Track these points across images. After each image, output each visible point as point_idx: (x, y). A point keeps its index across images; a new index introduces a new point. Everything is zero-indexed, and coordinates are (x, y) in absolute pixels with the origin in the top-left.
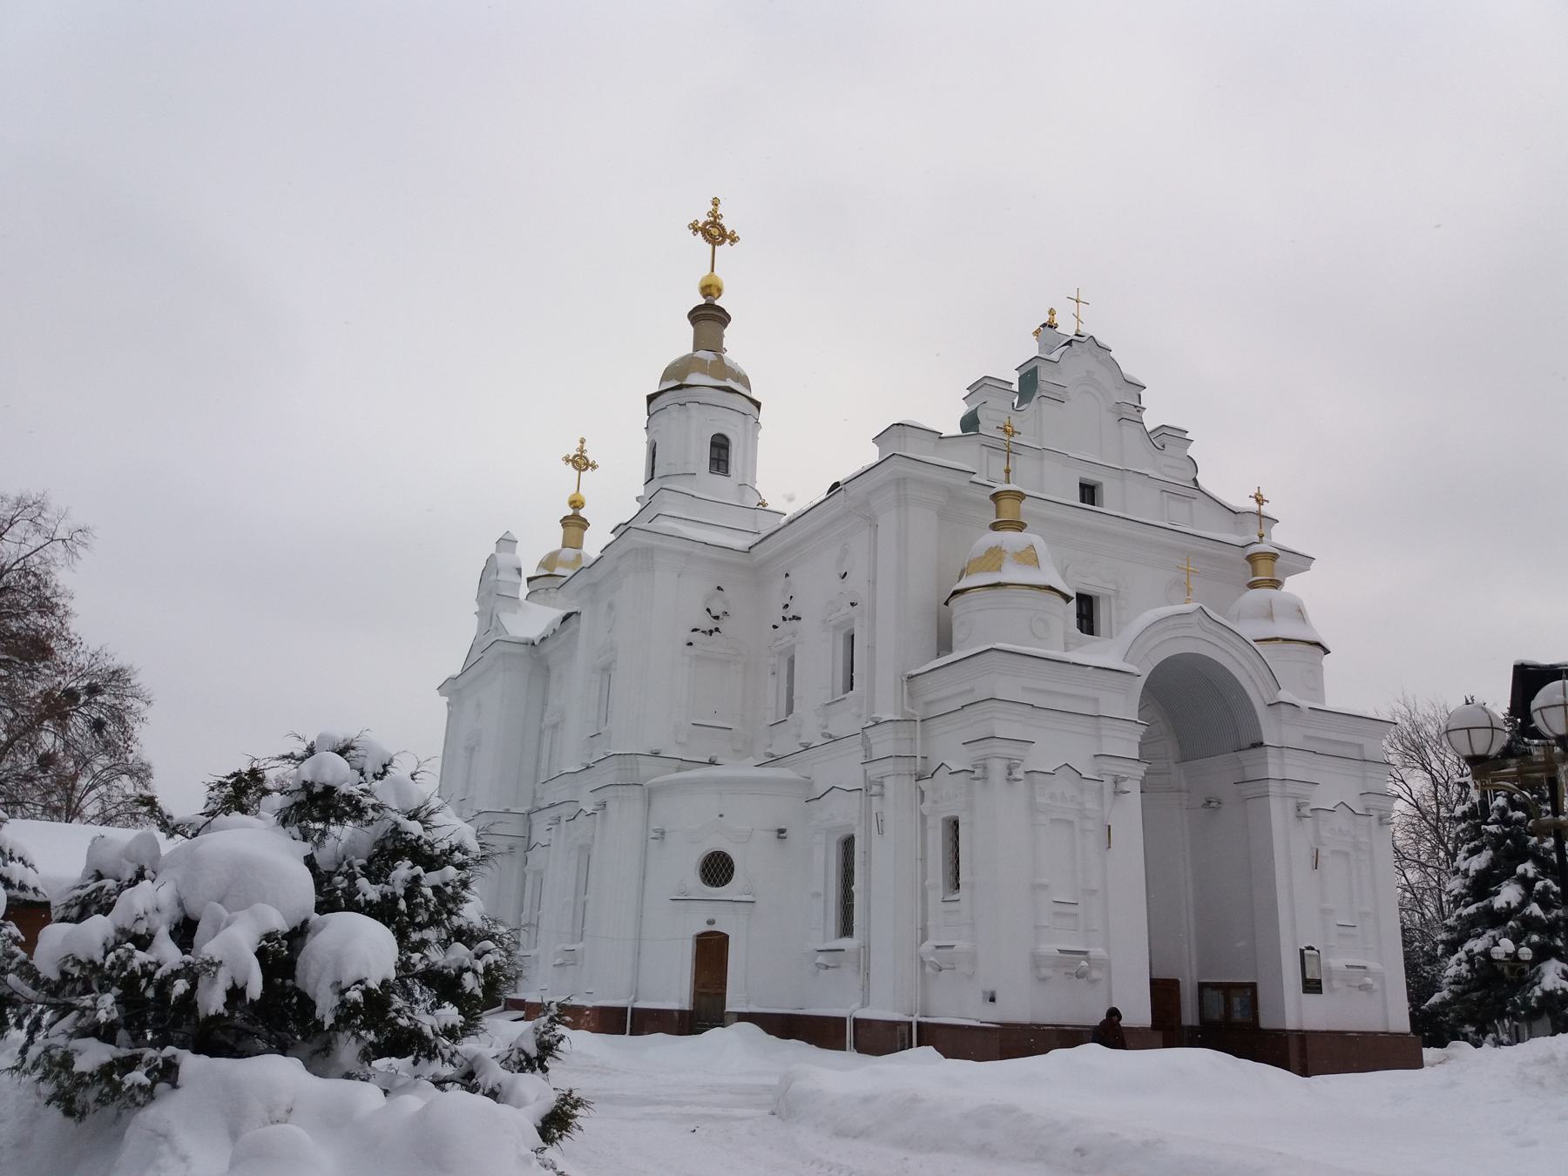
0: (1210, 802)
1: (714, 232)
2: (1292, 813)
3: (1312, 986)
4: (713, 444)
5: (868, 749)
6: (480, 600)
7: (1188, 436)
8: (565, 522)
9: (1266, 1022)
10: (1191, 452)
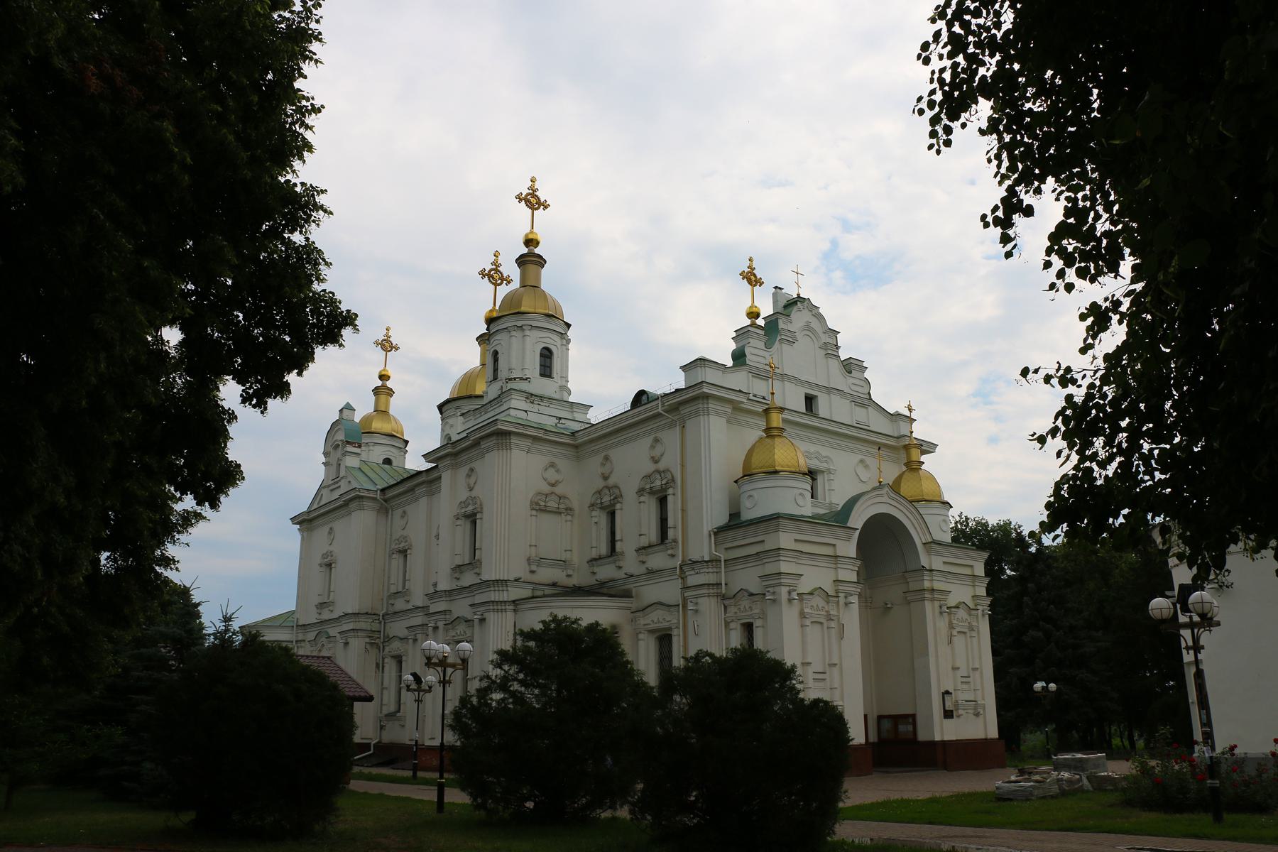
0: (887, 604)
1: (532, 201)
2: (937, 610)
3: (948, 714)
4: (542, 355)
6: (326, 454)
7: (865, 365)
8: (376, 391)
9: (922, 736)
10: (867, 375)
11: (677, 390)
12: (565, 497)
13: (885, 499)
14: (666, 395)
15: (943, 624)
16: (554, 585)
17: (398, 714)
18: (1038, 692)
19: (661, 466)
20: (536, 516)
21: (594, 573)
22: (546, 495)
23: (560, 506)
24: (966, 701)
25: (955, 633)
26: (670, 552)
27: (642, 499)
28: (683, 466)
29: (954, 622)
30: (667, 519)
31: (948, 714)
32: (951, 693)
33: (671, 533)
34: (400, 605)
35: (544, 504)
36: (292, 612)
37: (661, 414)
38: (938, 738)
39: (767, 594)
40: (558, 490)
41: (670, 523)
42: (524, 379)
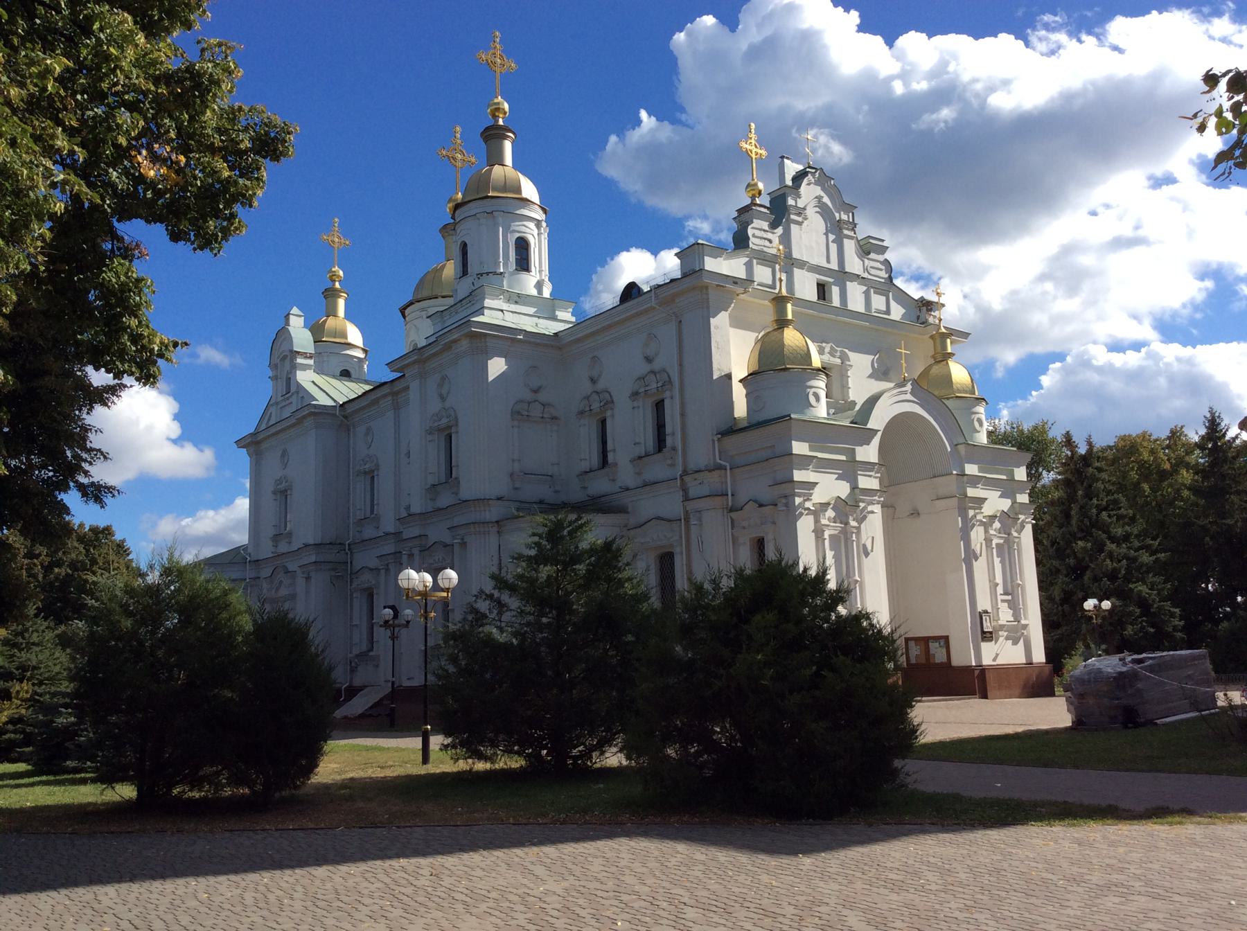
5: (685, 490)
6: (273, 366)
7: (885, 244)
9: (957, 661)
11: (672, 281)
12: (549, 405)
13: (909, 397)
14: (659, 286)
16: (541, 502)
17: (371, 654)
18: (1089, 611)
19: (656, 366)
20: (519, 427)
21: (585, 488)
22: (529, 403)
23: (545, 416)
26: (669, 462)
27: (636, 404)
28: (681, 365)
30: (664, 426)
33: (669, 441)
34: (369, 532)
36: (245, 548)
37: (654, 308)
39: (779, 504)
40: (542, 397)
41: (668, 429)
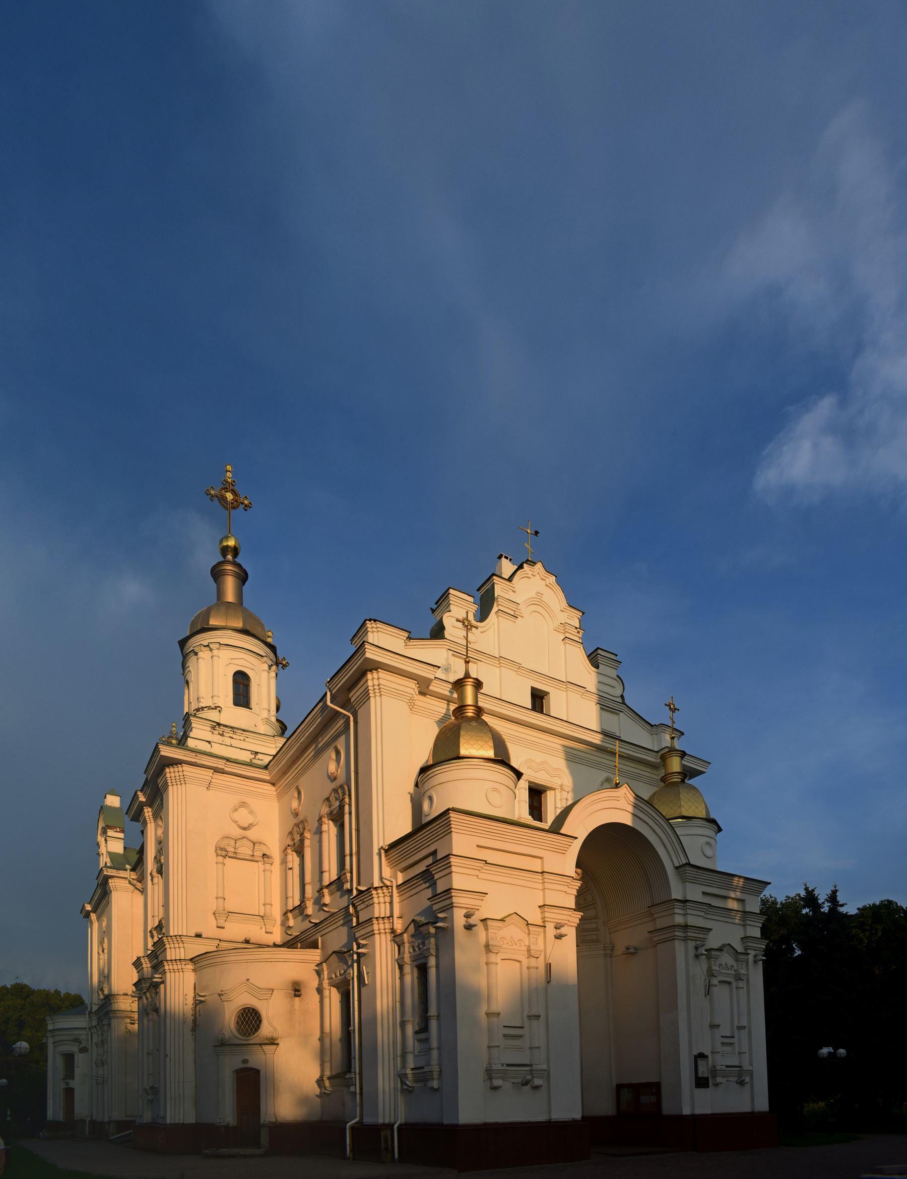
2: (692, 952)
9: (668, 1109)
15: (699, 970)
24: (727, 1066)
25: (715, 981)
29: (715, 968)
31: (701, 1083)
32: (707, 1057)
35: (233, 850)
38: (686, 1111)
42: (212, 709)
